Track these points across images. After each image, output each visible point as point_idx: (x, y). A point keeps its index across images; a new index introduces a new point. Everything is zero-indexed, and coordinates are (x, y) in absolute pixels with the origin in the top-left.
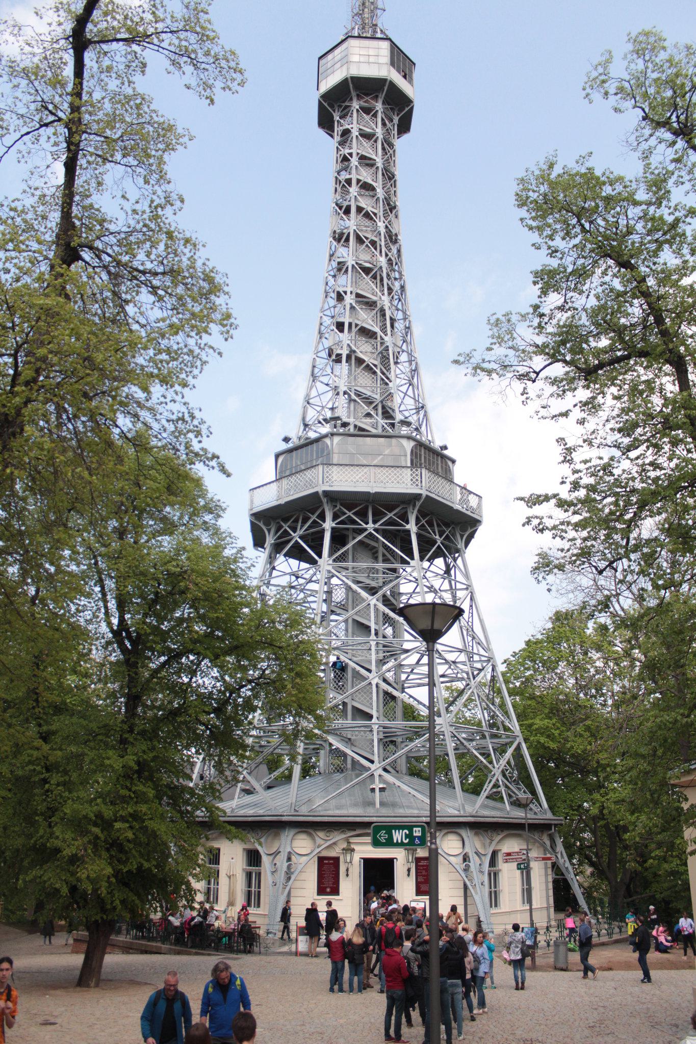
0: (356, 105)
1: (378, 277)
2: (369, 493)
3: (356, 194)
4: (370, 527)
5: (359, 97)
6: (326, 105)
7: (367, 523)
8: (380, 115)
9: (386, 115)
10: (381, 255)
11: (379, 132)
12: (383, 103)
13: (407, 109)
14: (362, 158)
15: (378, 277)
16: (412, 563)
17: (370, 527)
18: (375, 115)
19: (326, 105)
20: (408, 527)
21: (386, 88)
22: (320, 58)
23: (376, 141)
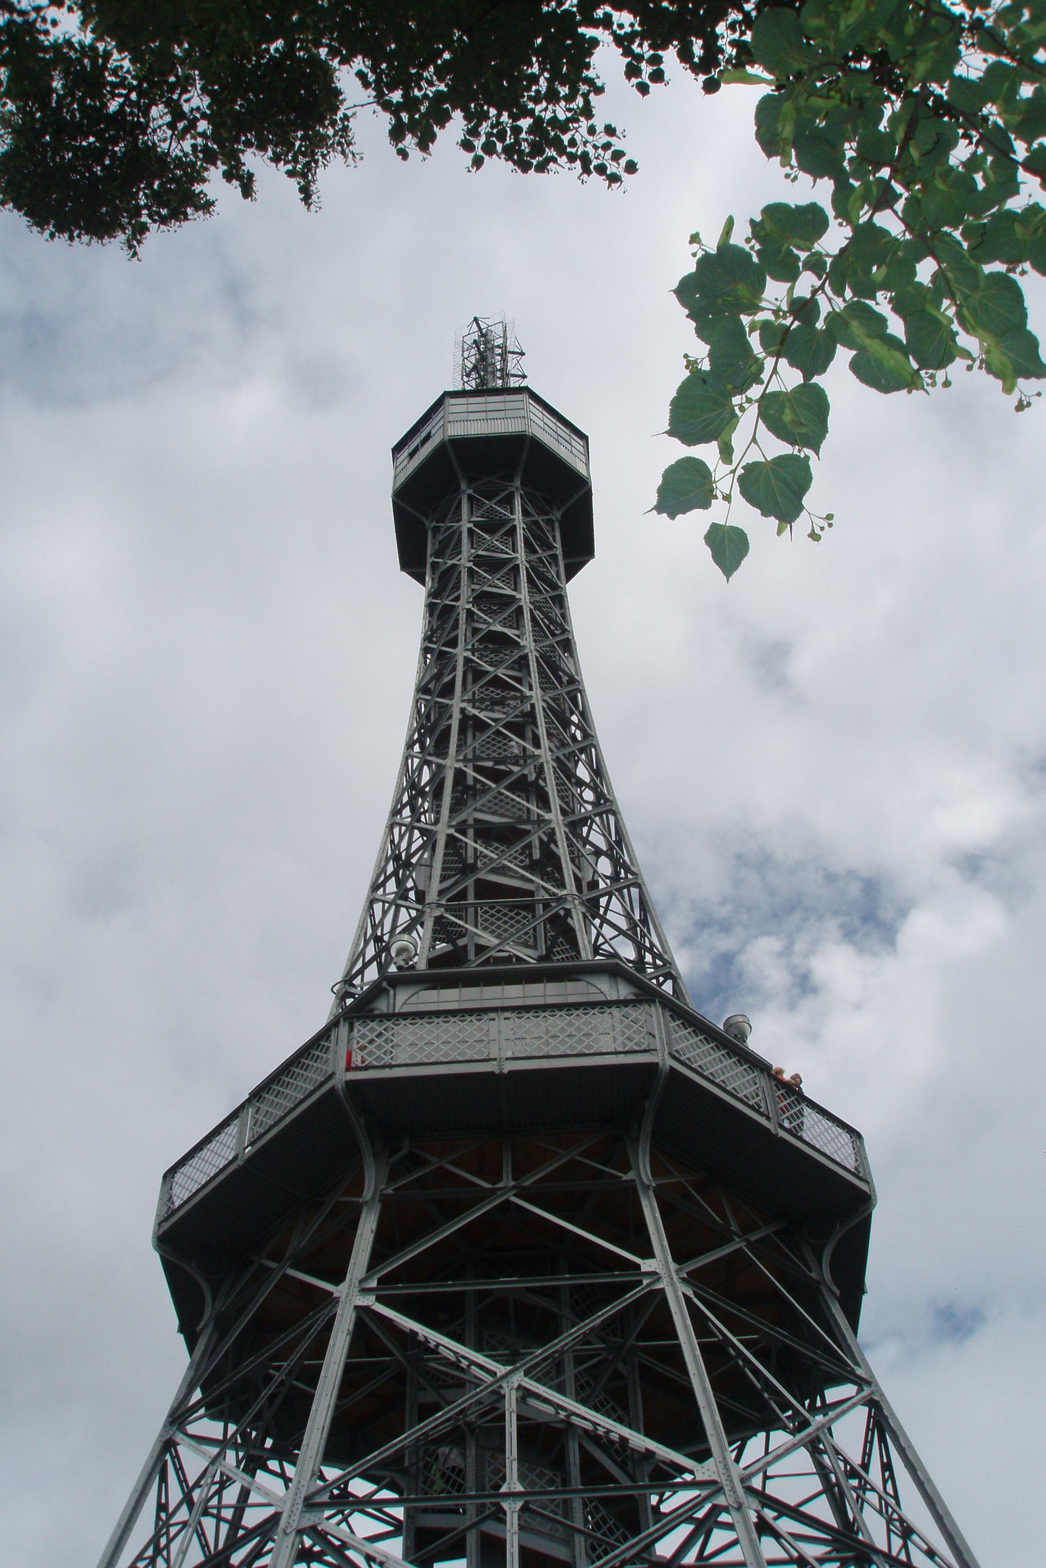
0: (467, 488)
1: (529, 734)
2: (493, 1073)
3: (470, 606)
4: (508, 1181)
5: (470, 481)
6: (409, 508)
7: (495, 1176)
8: (518, 503)
9: (535, 506)
10: (531, 689)
11: (518, 518)
12: (523, 483)
13: (575, 498)
14: (478, 560)
15: (529, 734)
16: (646, 1265)
17: (508, 1181)
18: (508, 501)
19: (409, 508)
20: (630, 1176)
21: (524, 456)
22: (397, 449)
23: (512, 531)
